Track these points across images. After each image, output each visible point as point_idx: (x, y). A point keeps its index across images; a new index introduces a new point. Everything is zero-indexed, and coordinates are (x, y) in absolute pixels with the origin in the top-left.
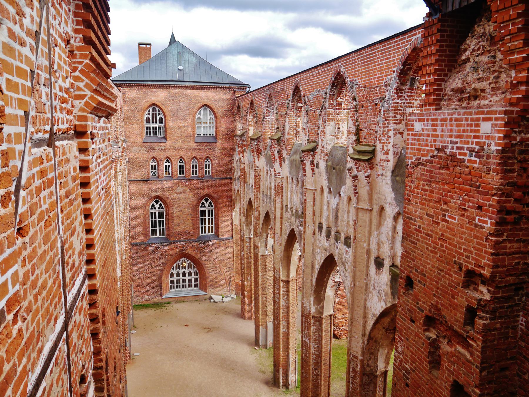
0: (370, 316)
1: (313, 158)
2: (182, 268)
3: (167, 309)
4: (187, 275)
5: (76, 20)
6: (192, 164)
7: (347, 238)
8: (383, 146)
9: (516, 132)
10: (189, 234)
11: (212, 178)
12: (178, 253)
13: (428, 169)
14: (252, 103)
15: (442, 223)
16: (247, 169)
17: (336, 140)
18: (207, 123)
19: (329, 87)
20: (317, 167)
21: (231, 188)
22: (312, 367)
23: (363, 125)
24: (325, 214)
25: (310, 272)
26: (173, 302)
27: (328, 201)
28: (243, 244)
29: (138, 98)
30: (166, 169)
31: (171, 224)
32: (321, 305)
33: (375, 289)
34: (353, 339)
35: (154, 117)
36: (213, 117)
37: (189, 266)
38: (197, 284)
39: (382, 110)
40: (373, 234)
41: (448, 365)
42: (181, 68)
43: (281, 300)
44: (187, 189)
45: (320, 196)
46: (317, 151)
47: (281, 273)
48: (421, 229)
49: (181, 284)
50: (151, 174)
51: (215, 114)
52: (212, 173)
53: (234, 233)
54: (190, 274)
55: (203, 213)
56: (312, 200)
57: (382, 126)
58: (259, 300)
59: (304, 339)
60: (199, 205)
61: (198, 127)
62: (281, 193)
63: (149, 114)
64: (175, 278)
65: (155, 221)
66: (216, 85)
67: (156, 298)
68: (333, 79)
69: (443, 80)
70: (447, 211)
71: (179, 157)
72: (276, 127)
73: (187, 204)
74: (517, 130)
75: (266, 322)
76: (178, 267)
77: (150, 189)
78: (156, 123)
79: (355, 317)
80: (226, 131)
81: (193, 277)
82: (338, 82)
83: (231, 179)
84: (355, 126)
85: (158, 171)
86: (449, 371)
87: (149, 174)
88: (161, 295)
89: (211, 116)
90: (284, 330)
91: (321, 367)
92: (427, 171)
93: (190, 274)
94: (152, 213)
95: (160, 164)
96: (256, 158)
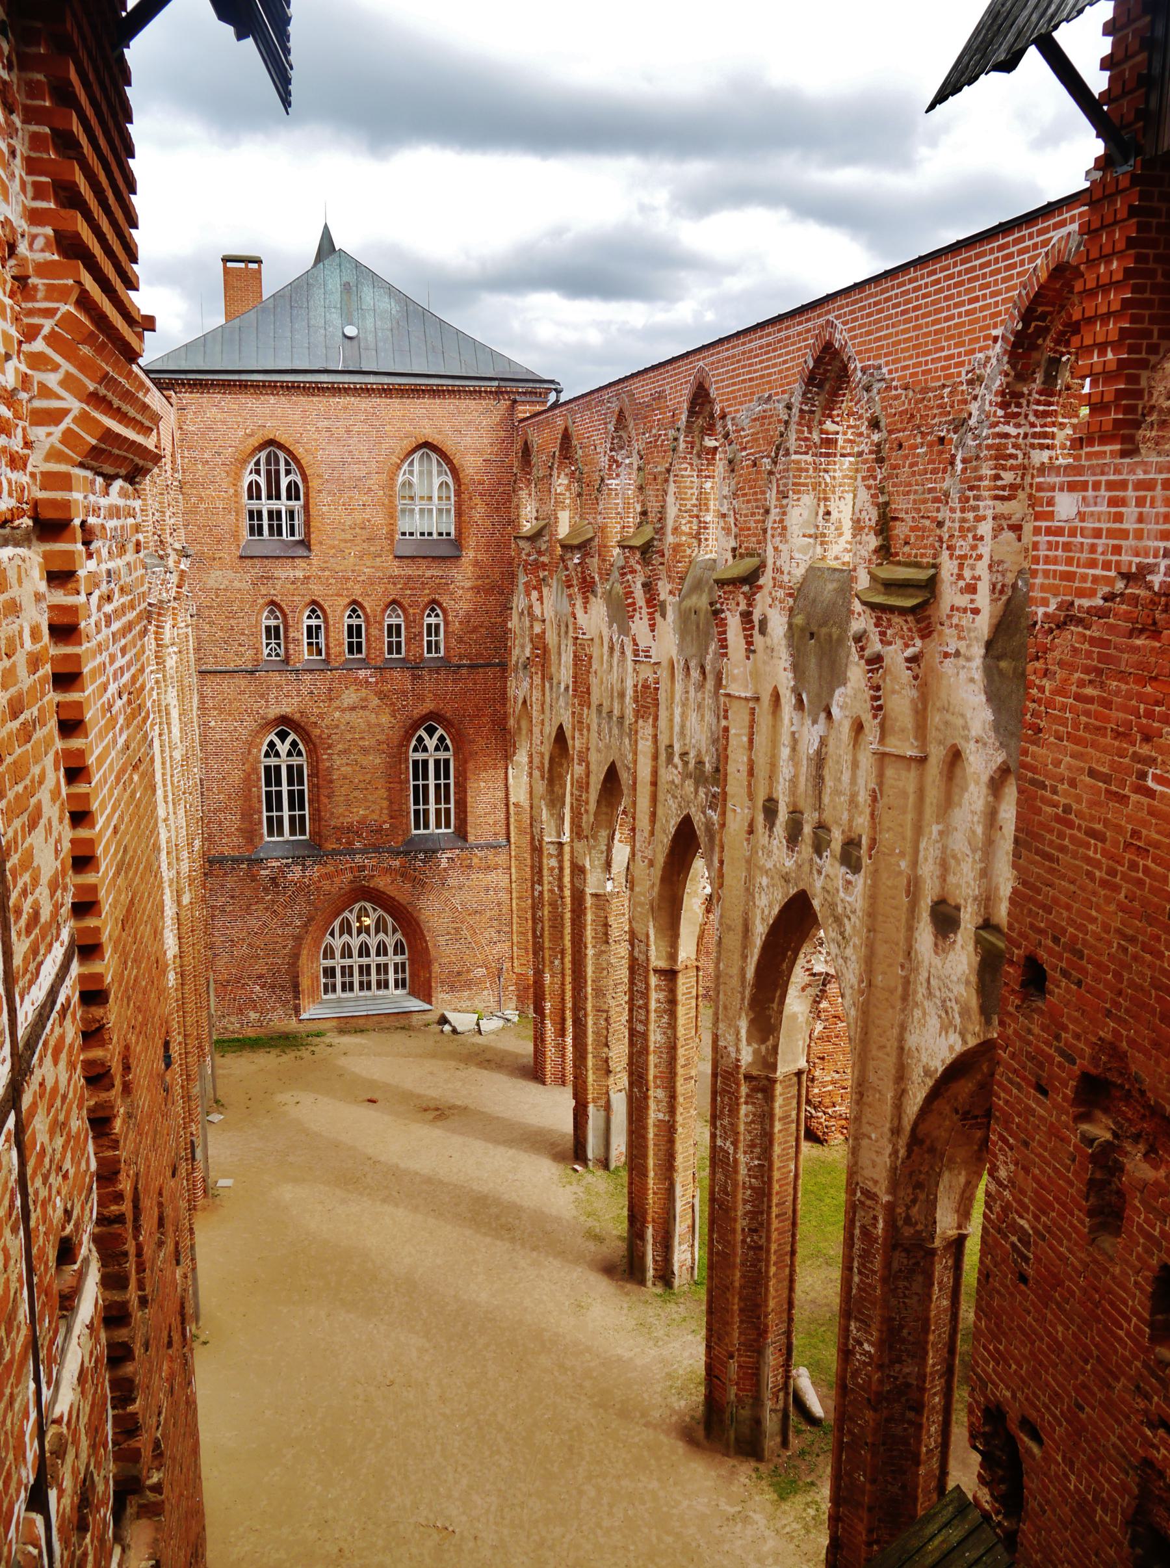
0: (916, 1074)
1: (749, 605)
2: (359, 932)
3: (313, 1053)
4: (373, 952)
5: (34, 184)
6: (388, 621)
7: (851, 844)
8: (961, 567)
10: (379, 830)
11: (445, 664)
12: (347, 889)
13: (1096, 634)
14: (566, 436)
15: (1134, 797)
16: (551, 638)
17: (819, 550)
18: (430, 498)
19: (798, 388)
20: (763, 632)
21: (505, 693)
22: (741, 1223)
23: (901, 505)
24: (785, 771)
25: (738, 944)
26: (330, 1030)
27: (793, 733)
28: (541, 863)
29: (224, 422)
30: (310, 636)
31: (326, 801)
32: (770, 1042)
33: (930, 995)
34: (865, 1142)
35: (273, 479)
36: (450, 481)
37: (380, 926)
38: (404, 980)
39: (959, 458)
40: (927, 830)
41: (1146, 1220)
42: (351, 331)
43: (652, 1026)
45: (770, 717)
46: (761, 582)
47: (653, 948)
48: (1072, 816)
49: (356, 979)
50: (266, 652)
51: (455, 471)
52: (446, 648)
53: (512, 828)
54: (382, 950)
55: (420, 769)
56: (746, 731)
57: (958, 506)
58: (585, 1026)
59: (719, 1142)
60: (408, 746)
61: (403, 511)
62: (652, 710)
63: (258, 472)
64: (338, 962)
65: (279, 793)
66: (458, 382)
67: (279, 1020)
68: (811, 364)
69: (1144, 364)
70: (1152, 761)
71: (348, 600)
72: (639, 509)
73: (373, 742)
75: (607, 1093)
76: (346, 928)
77: (262, 696)
78: (278, 498)
79: (872, 1077)
80: (488, 523)
81: (392, 959)
82: (827, 371)
83: (503, 666)
84: (878, 505)
85: (286, 642)
86: (1149, 1237)
87: (258, 651)
88: (297, 1010)
89: (444, 478)
90: (661, 1116)
91: (769, 1224)
92: (1093, 641)
93: (382, 950)
94: (267, 768)
95: (290, 622)
96: (579, 603)
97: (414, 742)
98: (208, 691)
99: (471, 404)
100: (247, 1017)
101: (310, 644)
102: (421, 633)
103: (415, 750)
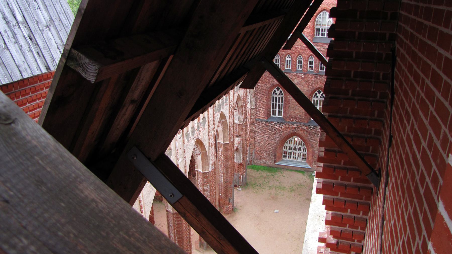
6: (310, 60)
10: (301, 118)
12: (291, 132)
18: (325, 25)
30: (287, 63)
38: (305, 159)
44: (303, 81)
54: (300, 149)
60: (312, 96)
64: (288, 151)
67: (270, 162)
85: (281, 64)
88: (275, 162)
93: (300, 149)
97: (314, 95)
100: (262, 161)
101: (287, 65)
103: (314, 97)
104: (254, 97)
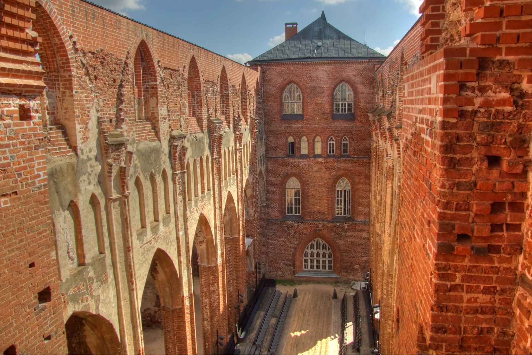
9: (473, 89)
10: (324, 214)
18: (345, 99)
29: (277, 76)
38: (331, 266)
44: (323, 168)
52: (350, 151)
54: (324, 255)
60: (335, 185)
62: (391, 177)
74: (475, 84)
76: (312, 247)
77: (286, 166)
87: (286, 151)
88: (294, 273)
97: (337, 184)
98: (269, 164)
99: (359, 65)
102: (341, 146)
104: (264, 191)
